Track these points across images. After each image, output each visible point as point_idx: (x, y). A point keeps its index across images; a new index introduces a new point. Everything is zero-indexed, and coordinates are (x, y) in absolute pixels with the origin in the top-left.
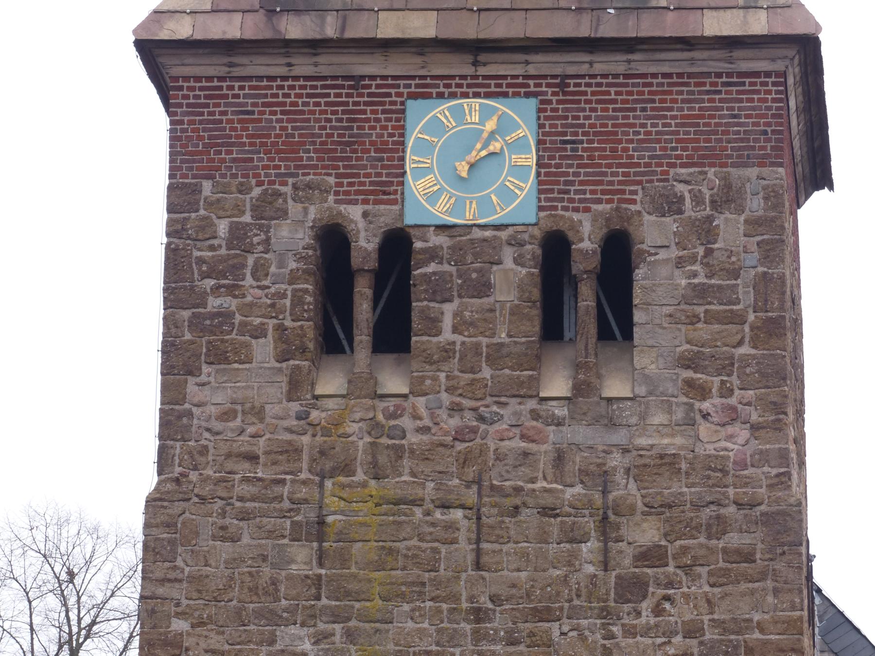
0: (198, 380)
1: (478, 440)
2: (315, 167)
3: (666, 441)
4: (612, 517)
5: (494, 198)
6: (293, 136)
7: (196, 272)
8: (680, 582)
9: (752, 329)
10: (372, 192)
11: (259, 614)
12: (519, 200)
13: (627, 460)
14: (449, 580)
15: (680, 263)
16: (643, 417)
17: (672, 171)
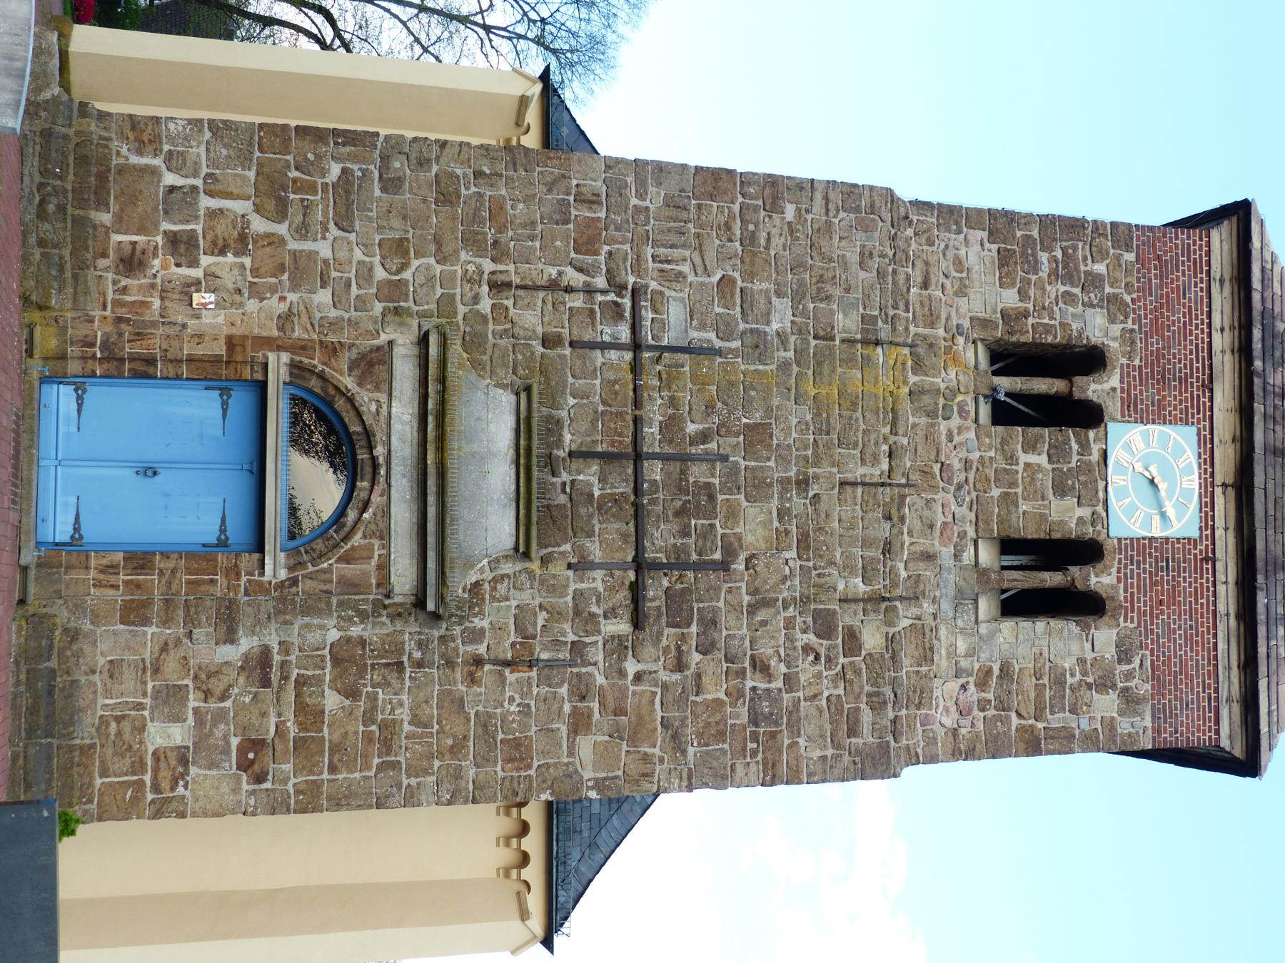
0: (986, 240)
1: (942, 484)
2: (1146, 350)
3: (944, 652)
4: (883, 605)
5: (1127, 501)
6: (1168, 331)
7: (1067, 244)
8: (830, 669)
9: (1031, 726)
10: (1129, 395)
11: (801, 283)
12: (1126, 521)
13: (929, 621)
14: (831, 456)
15: (1082, 661)
16: (963, 631)
17: (1148, 653)
